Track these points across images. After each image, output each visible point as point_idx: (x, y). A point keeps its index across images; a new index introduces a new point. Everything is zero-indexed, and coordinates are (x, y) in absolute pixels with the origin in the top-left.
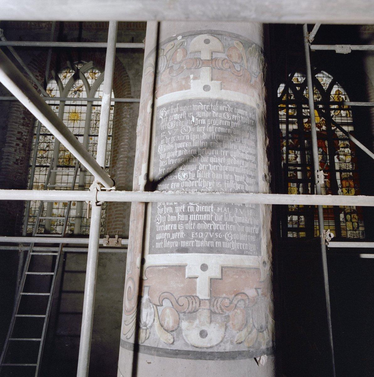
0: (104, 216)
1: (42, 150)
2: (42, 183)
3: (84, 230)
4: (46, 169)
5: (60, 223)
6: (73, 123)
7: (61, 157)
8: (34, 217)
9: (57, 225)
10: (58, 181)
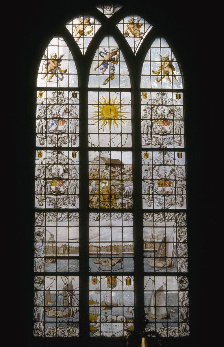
0: (187, 302)
1: (55, 178)
2: (64, 244)
4: (68, 215)
5: (106, 317)
6: (108, 125)
7: (93, 193)
8: (57, 306)
9: (101, 322)
10: (93, 238)
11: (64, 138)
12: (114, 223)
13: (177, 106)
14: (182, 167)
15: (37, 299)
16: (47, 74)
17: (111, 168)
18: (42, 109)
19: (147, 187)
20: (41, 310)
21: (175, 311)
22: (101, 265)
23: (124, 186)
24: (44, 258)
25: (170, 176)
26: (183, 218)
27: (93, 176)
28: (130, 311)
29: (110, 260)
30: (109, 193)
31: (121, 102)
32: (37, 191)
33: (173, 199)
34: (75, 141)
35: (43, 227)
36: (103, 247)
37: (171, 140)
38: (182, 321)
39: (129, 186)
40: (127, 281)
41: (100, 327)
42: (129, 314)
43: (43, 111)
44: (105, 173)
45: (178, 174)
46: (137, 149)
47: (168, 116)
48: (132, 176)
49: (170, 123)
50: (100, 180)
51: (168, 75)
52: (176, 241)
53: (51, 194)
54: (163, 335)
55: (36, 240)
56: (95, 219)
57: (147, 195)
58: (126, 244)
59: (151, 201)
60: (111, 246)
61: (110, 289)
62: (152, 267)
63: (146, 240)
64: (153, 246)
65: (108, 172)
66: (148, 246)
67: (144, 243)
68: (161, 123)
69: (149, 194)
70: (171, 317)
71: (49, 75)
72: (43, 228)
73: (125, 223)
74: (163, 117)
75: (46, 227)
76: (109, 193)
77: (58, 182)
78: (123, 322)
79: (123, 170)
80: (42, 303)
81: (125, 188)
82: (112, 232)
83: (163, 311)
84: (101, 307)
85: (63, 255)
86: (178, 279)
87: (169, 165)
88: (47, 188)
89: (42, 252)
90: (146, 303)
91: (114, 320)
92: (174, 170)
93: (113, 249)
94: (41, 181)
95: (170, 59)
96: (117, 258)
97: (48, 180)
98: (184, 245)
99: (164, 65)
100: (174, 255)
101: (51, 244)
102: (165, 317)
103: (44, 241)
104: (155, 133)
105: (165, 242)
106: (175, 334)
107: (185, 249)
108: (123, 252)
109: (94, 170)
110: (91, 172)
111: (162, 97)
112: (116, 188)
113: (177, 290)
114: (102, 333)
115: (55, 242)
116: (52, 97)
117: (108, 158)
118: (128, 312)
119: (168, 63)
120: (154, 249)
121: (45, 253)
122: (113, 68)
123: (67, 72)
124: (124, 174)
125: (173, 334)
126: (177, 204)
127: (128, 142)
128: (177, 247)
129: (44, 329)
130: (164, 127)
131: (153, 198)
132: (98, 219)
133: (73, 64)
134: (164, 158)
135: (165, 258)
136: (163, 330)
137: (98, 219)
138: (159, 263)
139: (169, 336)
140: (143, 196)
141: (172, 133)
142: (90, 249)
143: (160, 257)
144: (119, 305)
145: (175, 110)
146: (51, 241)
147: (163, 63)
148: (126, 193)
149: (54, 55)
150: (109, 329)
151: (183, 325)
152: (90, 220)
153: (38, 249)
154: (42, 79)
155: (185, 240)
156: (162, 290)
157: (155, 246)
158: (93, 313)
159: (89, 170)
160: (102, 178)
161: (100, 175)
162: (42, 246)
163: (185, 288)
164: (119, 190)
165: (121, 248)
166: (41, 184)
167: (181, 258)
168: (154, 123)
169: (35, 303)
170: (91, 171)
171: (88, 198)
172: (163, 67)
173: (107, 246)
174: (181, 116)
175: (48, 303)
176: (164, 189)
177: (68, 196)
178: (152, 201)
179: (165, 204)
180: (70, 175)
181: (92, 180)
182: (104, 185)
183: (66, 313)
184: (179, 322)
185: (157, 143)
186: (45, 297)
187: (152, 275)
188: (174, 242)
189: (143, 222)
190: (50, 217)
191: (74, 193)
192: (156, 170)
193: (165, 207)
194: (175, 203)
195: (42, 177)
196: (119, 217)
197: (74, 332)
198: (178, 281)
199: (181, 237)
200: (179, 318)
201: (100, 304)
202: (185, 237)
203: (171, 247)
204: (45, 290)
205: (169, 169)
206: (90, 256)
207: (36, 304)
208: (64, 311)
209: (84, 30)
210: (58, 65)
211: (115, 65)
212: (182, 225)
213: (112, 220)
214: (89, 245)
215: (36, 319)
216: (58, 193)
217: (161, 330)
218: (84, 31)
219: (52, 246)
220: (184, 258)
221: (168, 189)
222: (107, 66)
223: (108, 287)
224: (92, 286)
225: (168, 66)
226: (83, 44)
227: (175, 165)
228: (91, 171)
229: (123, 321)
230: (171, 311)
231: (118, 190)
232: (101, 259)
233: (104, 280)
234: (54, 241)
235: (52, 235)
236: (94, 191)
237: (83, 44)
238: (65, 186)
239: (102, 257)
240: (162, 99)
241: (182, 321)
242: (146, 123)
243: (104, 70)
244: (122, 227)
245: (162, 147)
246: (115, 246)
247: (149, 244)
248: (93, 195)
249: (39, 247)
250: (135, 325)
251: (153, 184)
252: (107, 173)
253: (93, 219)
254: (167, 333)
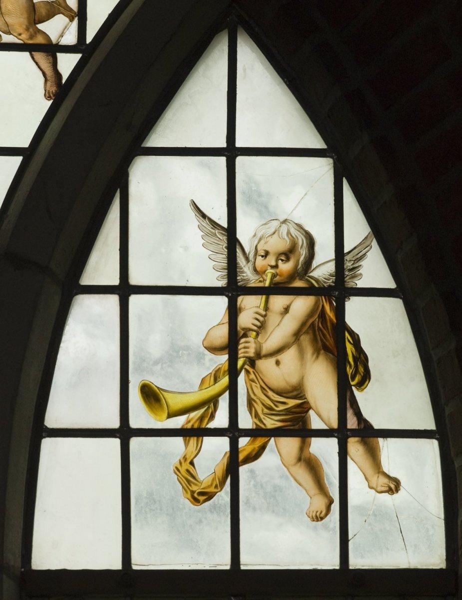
51: (297, 426)
99: (262, 327)
119: (302, 305)
147: (250, 305)
172: (248, 347)
225: (297, 335)
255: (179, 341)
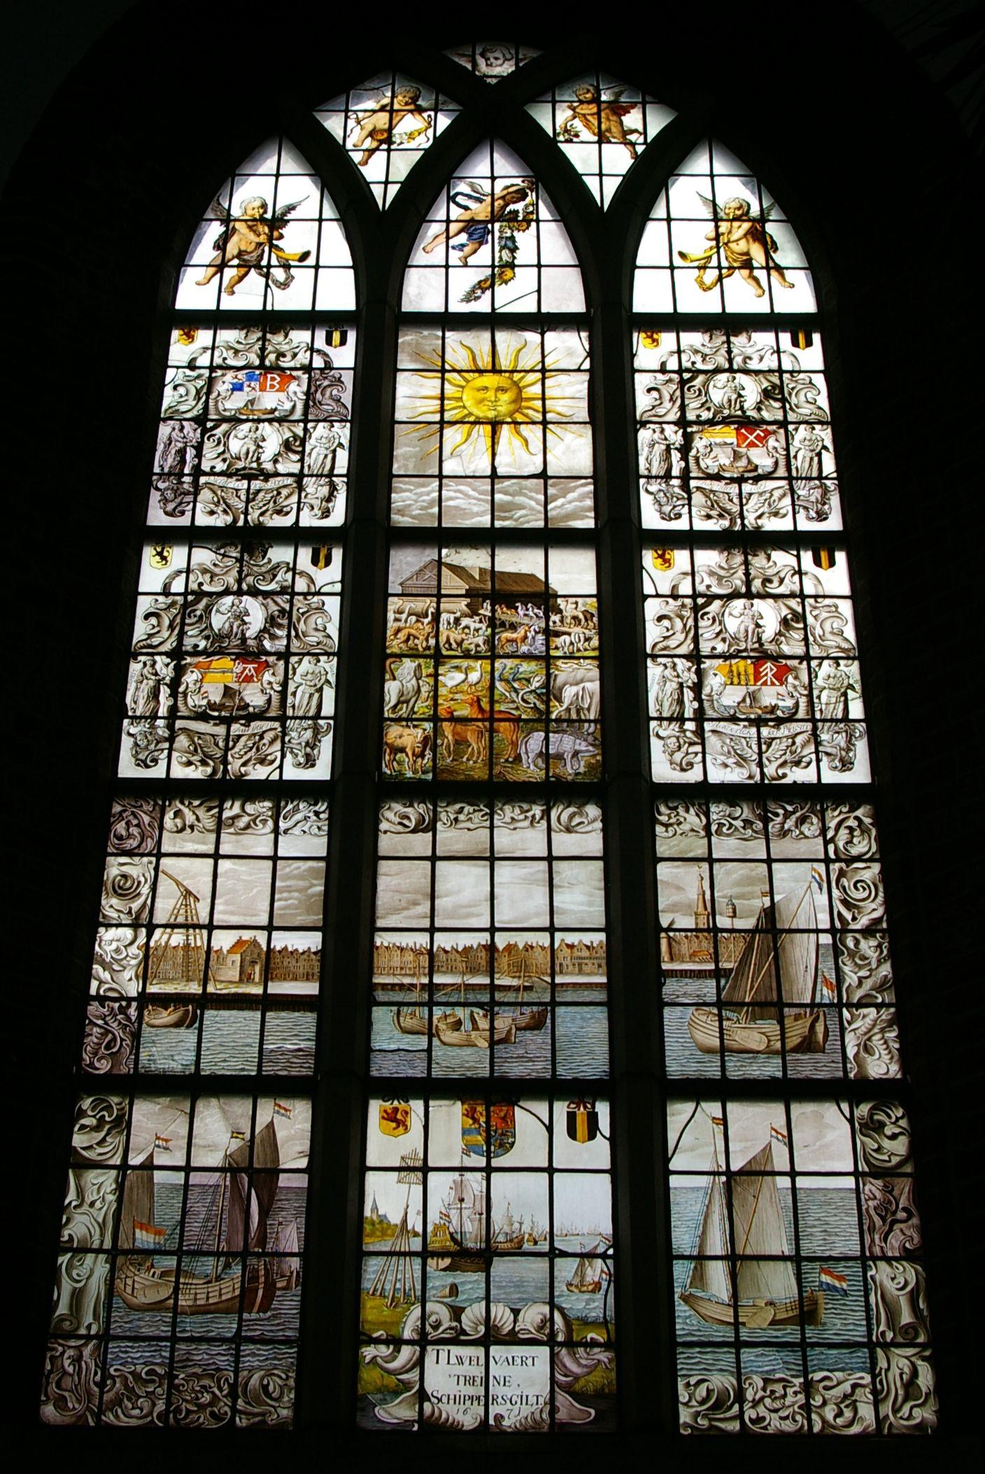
2: (247, 935)
3: (722, 1381)
5: (457, 1313)
7: (404, 711)
9: (423, 1341)
10: (397, 910)
11: (279, 493)
12: (505, 841)
13: (800, 372)
14: (836, 607)
15: (79, 1211)
16: (220, 267)
17: (493, 611)
18: (190, 386)
19: (672, 686)
20: (95, 1270)
21: (845, 1285)
22: (435, 1040)
23: (560, 681)
24: (133, 999)
25: (783, 639)
26: (857, 818)
27: (408, 640)
28: (588, 1279)
29: (485, 1016)
30: (481, 709)
31: (543, 362)
32: (135, 703)
33: (799, 740)
34: (330, 505)
35: (149, 854)
36: (446, 952)
37: (780, 499)
38: (890, 1336)
39: (581, 684)
40: (571, 1117)
41: (417, 1371)
42: (587, 1296)
43: (193, 392)
44: (467, 627)
45: (818, 631)
46: (618, 540)
47: (759, 410)
48: (595, 642)
49: (768, 433)
50: (438, 658)
51: (748, 264)
52: (827, 926)
53: (202, 717)
54: (786, 1418)
55: (105, 916)
56: (412, 825)
57: (670, 719)
58: (572, 938)
59: (691, 744)
60: (491, 948)
61: (482, 1162)
62: (708, 1051)
63: (672, 923)
64: (712, 950)
65: (478, 625)
66: (685, 949)
67: (663, 935)
68: (728, 435)
69: (681, 719)
70: (823, 1317)
71: (229, 273)
72: (145, 859)
73: (564, 843)
74: (739, 413)
75: (159, 855)
76: (481, 709)
77: (238, 667)
78: (551, 1342)
79: (555, 618)
80: (102, 1235)
81: (561, 689)
82: (500, 889)
83: (779, 1284)
84: (425, 1254)
85: (240, 991)
86: (857, 1113)
87: (776, 597)
88: (181, 689)
89: (129, 973)
90: (683, 1238)
91: (498, 1329)
92: (801, 617)
93: (503, 962)
94: (155, 662)
95: (755, 211)
96: (522, 1004)
97: (189, 660)
98: (873, 943)
99: (730, 232)
100: (825, 991)
101: (177, 938)
102: (791, 1314)
103: (144, 922)
104: (701, 475)
105: (771, 929)
106: (856, 1411)
107: (879, 963)
108: (553, 979)
109: (414, 618)
110: (397, 624)
111: (728, 342)
112: (516, 691)
113: (851, 1169)
114: (427, 1406)
115: (201, 927)
116: (238, 342)
117: (480, 569)
118: (579, 1285)
119: (746, 226)
120: (717, 965)
121: (145, 977)
122: (510, 244)
123: (311, 261)
124: (558, 634)
125: (840, 1414)
126: (825, 759)
127: (577, 507)
128: (837, 953)
129: (98, 1378)
130: (743, 450)
131: (700, 732)
132: (428, 826)
133: (334, 235)
134: (747, 570)
135: (772, 1006)
136: (785, 1387)
137: (428, 826)
138: (745, 1033)
139: (817, 1428)
140: (653, 724)
141: (782, 472)
142: (380, 961)
143: (748, 1004)
144: (527, 1246)
145: (793, 389)
146: (181, 920)
148: (568, 710)
149: (258, 203)
150: (470, 1381)
151: (899, 1363)
152: (384, 826)
153: (108, 959)
154: (198, 284)
155: (877, 921)
156: (768, 1168)
157: (721, 950)
158: (379, 1287)
159: (391, 616)
160: (451, 649)
161: (443, 639)
162: (132, 943)
163: (895, 1160)
164: (532, 699)
165: (543, 959)
166: (156, 674)
167: (860, 1005)
168: (697, 437)
169: (66, 1233)
170: (396, 620)
171: (380, 733)
172: (723, 239)
173: (472, 947)
174: (820, 408)
175: (138, 1231)
176: (753, 697)
177: (283, 726)
178: (698, 748)
179: (764, 760)
180: (297, 636)
181: (400, 656)
182: (459, 677)
183: (230, 1287)
184: (871, 1346)
185: (713, 513)
186: (120, 1201)
187: (710, 1097)
188: (817, 931)
189: (654, 836)
190: (186, 810)
191: (311, 714)
192: (710, 616)
193: (762, 773)
194: (813, 756)
195: (161, 643)
196: (533, 816)
197: (269, 1395)
198: (851, 1121)
199: (858, 907)
200: (868, 1319)
201: (419, 1240)
202: (873, 906)
203: (803, 955)
204: (124, 1167)
205: (770, 615)
206: (381, 996)
207: (66, 1238)
208: (218, 1278)
209: (391, 128)
210: (270, 238)
211: (515, 233)
212: (854, 851)
213: (496, 830)
214: (378, 942)
215: (62, 1319)
216: (231, 711)
217: (773, 1392)
218: (394, 132)
219: (187, 946)
220: (879, 1007)
221: (770, 696)
222: (483, 236)
223: (469, 1149)
224: (382, 1145)
225: (745, 235)
226: (383, 174)
227: (802, 596)
228: (396, 620)
229: (552, 1334)
230: (821, 1282)
231: (523, 700)
232: (438, 1012)
233: (449, 1117)
234: (195, 921)
235: (188, 893)
236: (407, 702)
237: (383, 174)
238: (270, 683)
239: (444, 999)
240: (729, 347)
241: (890, 1336)
242: (657, 436)
243: (467, 250)
244: (550, 859)
245: (738, 528)
246: (510, 948)
247: (686, 937)
248: (410, 720)
249: (117, 951)
250: (619, 1360)
251: (700, 673)
252: (477, 630)
253: (400, 823)
254: (807, 1408)
255: (695, 239)
